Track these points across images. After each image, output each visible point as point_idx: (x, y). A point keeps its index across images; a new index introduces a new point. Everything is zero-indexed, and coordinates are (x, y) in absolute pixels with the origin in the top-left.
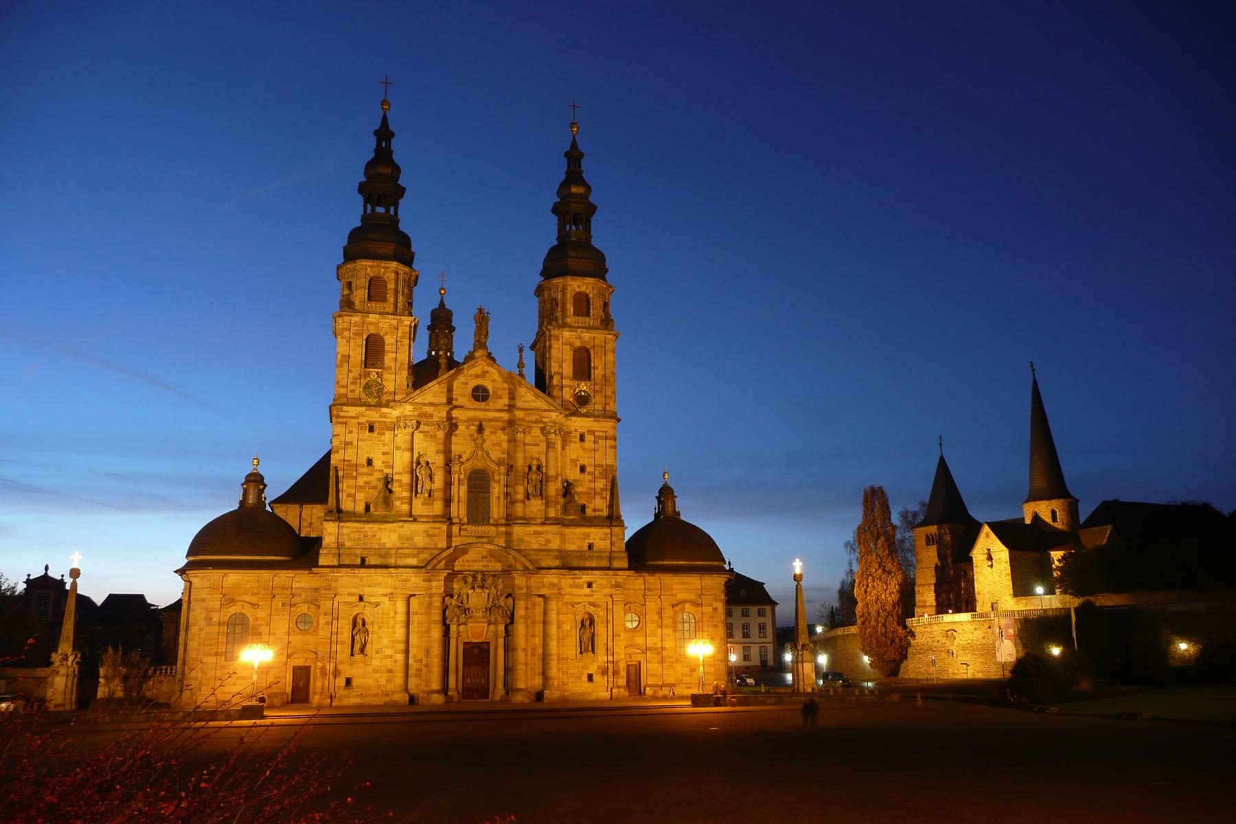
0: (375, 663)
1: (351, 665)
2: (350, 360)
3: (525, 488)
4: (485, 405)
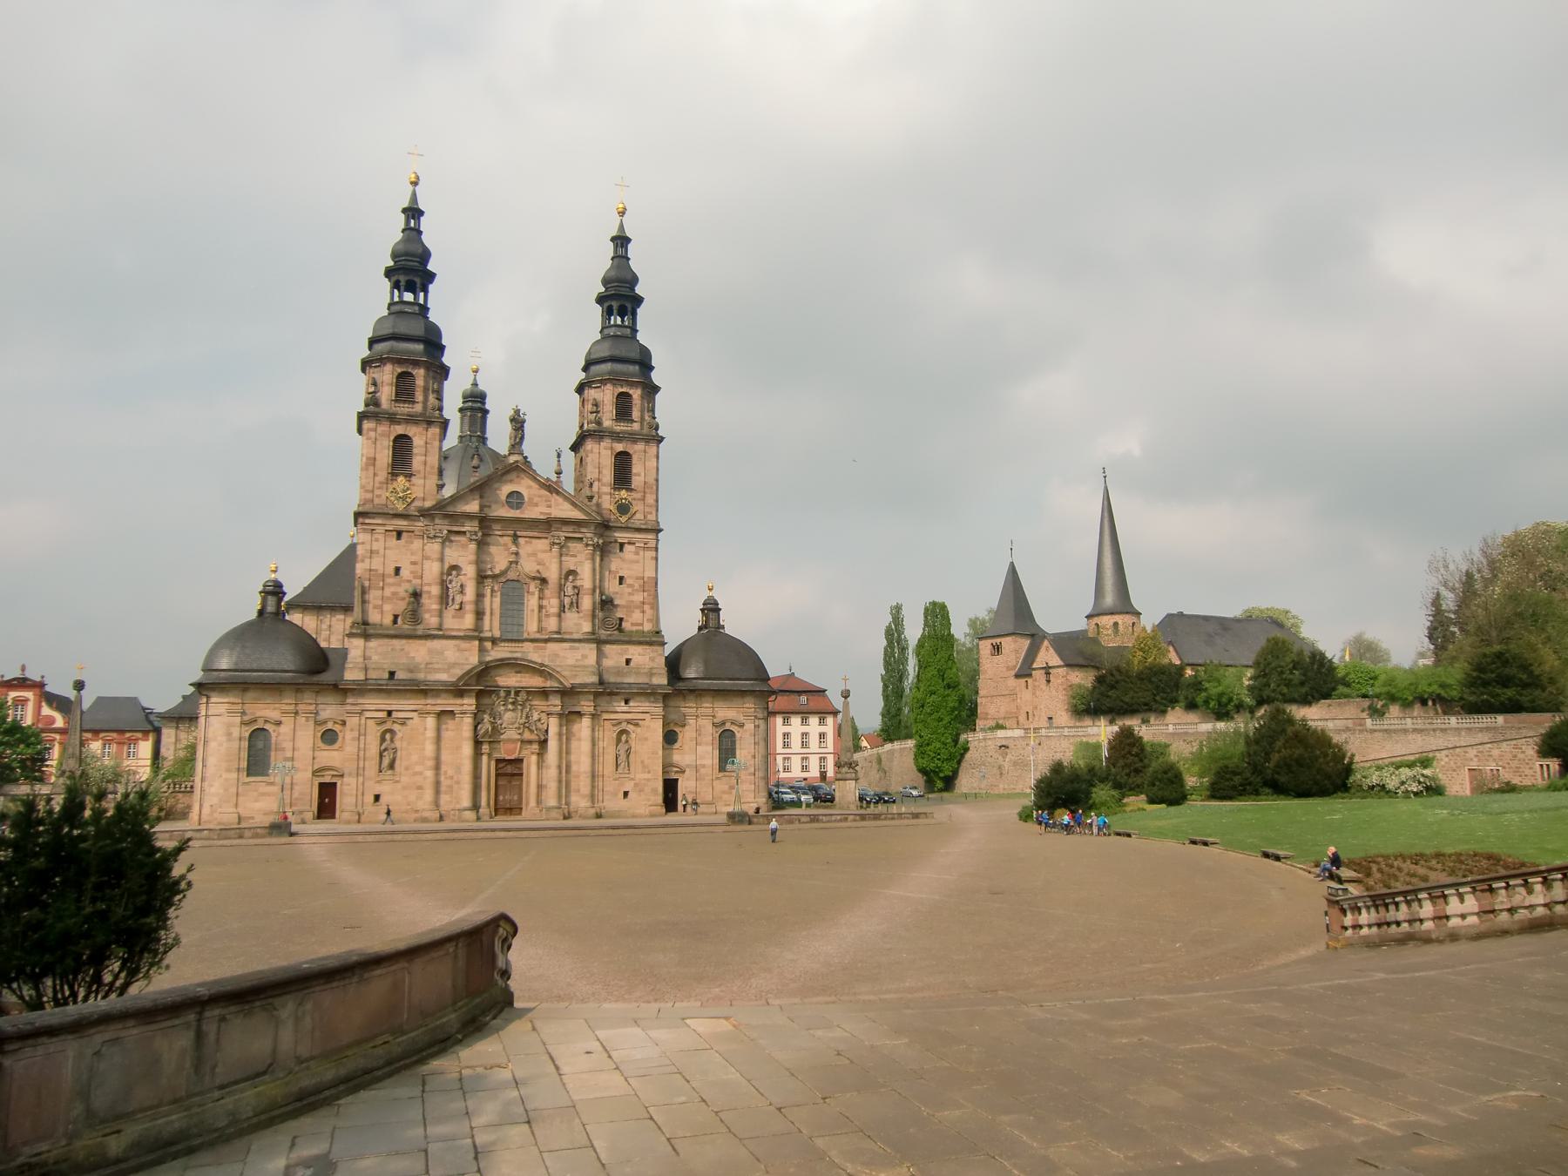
0: (404, 779)
1: (379, 782)
2: (377, 463)
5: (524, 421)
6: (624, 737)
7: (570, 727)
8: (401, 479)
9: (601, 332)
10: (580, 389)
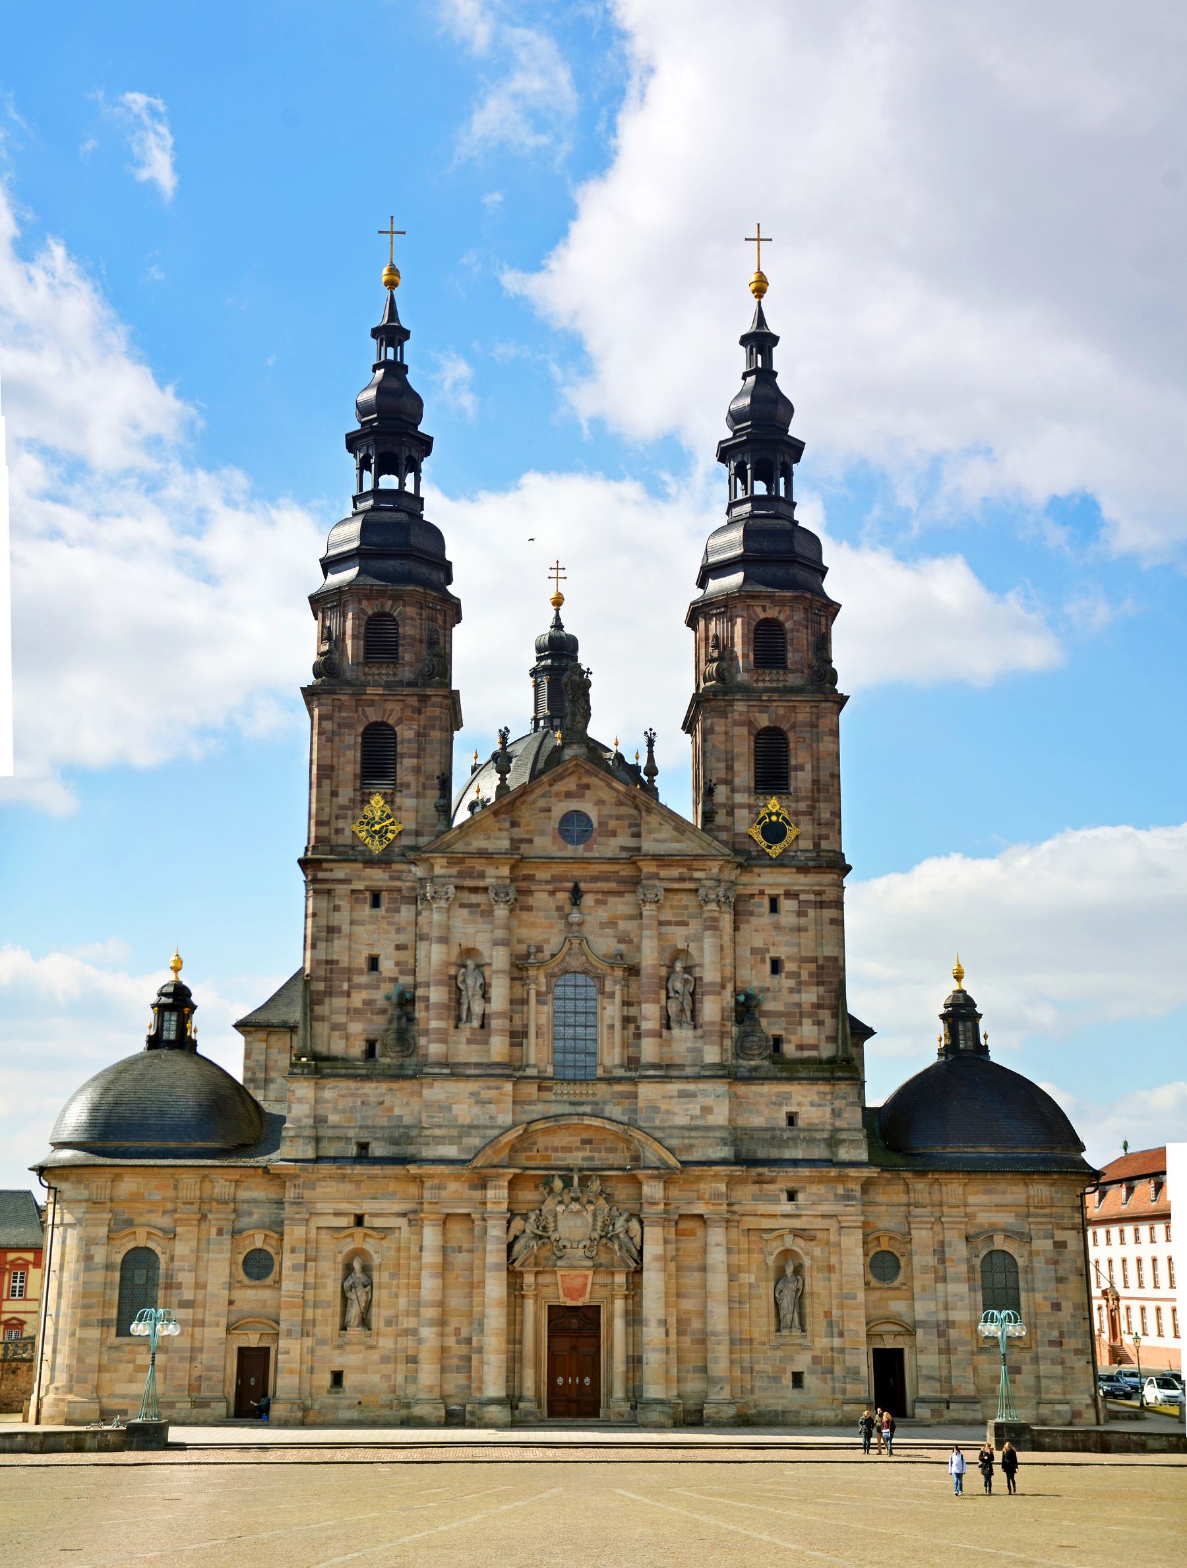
0: (386, 1343)
1: (340, 1347)
3: (661, 1007)
4: (585, 850)
6: (789, 1270)
7: (682, 1245)
8: (377, 801)
9: (728, 514)
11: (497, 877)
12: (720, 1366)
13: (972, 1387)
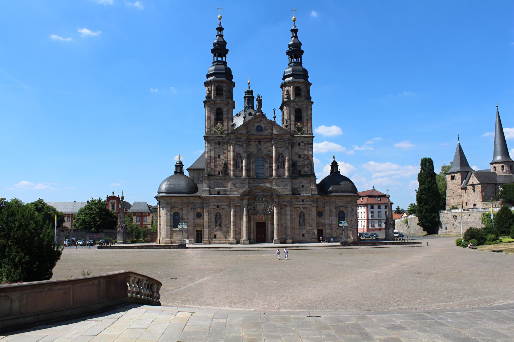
5: (261, 100)
6: (302, 215)
8: (219, 124)
10: (283, 86)
11: (244, 139)
12: (289, 233)
13: (336, 235)
